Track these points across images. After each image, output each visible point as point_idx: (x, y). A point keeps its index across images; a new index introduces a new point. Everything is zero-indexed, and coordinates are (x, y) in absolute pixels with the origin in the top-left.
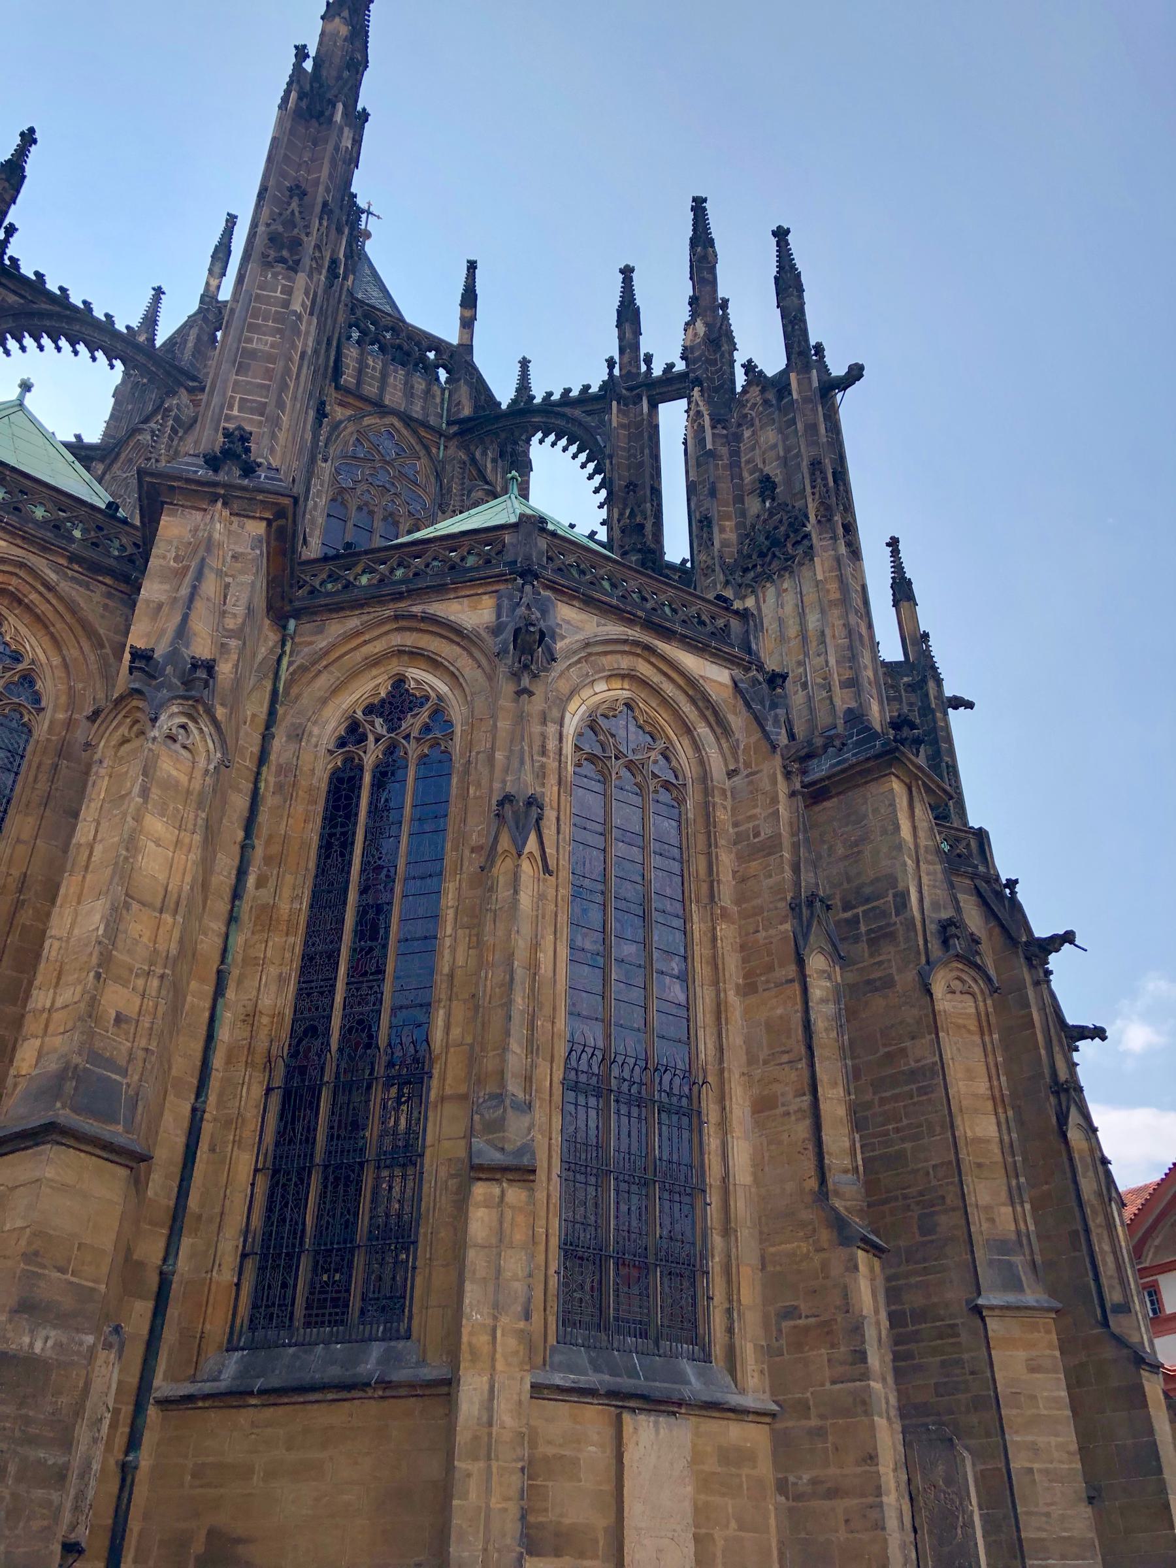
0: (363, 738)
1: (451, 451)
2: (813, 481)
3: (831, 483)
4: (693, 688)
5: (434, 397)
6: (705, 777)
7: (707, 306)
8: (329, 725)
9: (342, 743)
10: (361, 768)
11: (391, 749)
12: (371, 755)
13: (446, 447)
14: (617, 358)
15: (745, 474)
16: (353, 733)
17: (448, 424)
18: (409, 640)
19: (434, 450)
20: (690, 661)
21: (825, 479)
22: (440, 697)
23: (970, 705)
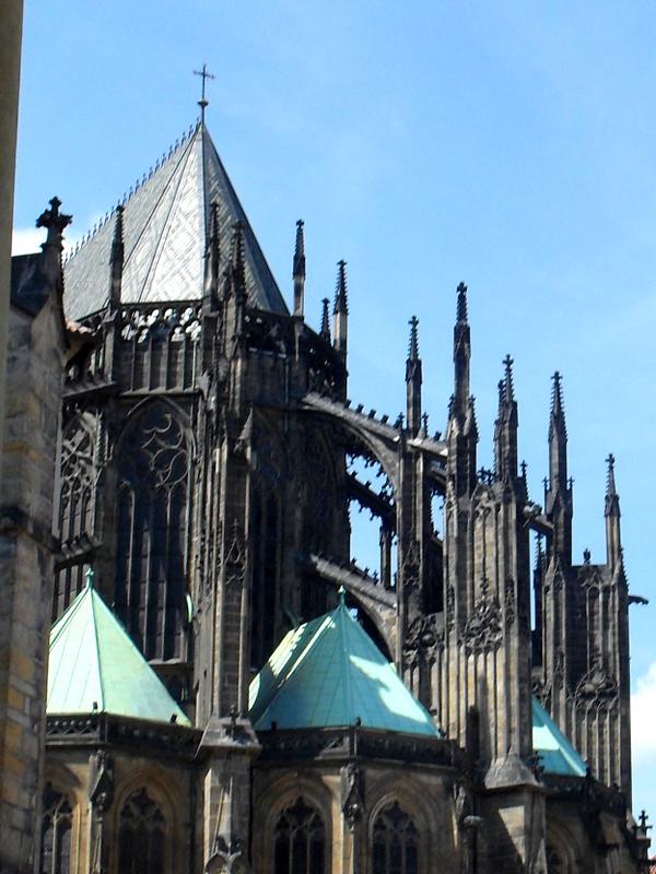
0: (287, 826)
1: (293, 422)
2: (506, 592)
3: (516, 596)
4: (425, 789)
5: (278, 371)
6: (429, 831)
7: (460, 405)
8: (273, 817)
9: (279, 826)
10: (288, 839)
11: (300, 833)
12: (292, 835)
13: (289, 419)
14: (405, 414)
15: (476, 557)
16: (283, 825)
17: (290, 398)
18: (303, 781)
19: (280, 423)
20: (424, 778)
21: (513, 591)
22: (318, 810)
23: (645, 602)
